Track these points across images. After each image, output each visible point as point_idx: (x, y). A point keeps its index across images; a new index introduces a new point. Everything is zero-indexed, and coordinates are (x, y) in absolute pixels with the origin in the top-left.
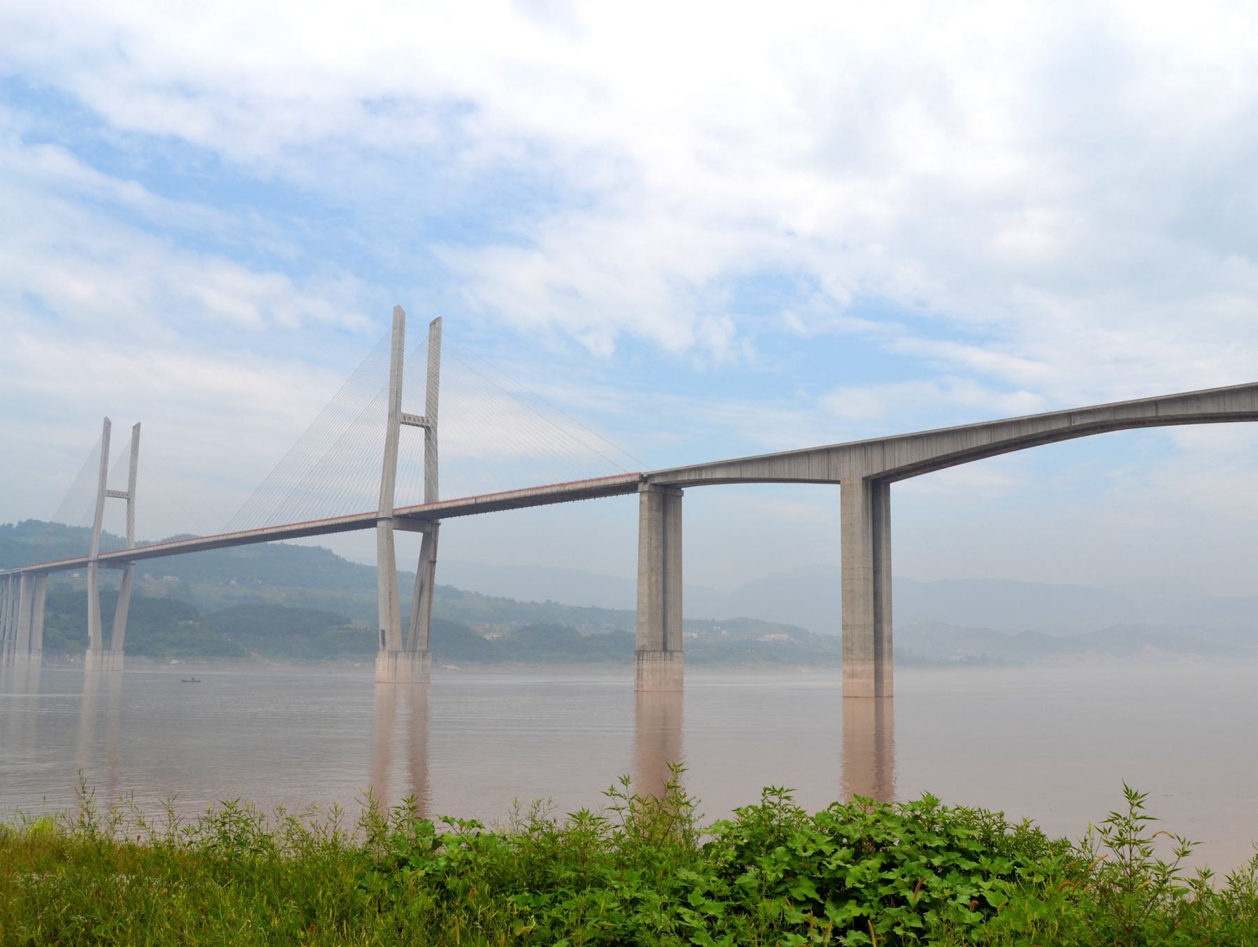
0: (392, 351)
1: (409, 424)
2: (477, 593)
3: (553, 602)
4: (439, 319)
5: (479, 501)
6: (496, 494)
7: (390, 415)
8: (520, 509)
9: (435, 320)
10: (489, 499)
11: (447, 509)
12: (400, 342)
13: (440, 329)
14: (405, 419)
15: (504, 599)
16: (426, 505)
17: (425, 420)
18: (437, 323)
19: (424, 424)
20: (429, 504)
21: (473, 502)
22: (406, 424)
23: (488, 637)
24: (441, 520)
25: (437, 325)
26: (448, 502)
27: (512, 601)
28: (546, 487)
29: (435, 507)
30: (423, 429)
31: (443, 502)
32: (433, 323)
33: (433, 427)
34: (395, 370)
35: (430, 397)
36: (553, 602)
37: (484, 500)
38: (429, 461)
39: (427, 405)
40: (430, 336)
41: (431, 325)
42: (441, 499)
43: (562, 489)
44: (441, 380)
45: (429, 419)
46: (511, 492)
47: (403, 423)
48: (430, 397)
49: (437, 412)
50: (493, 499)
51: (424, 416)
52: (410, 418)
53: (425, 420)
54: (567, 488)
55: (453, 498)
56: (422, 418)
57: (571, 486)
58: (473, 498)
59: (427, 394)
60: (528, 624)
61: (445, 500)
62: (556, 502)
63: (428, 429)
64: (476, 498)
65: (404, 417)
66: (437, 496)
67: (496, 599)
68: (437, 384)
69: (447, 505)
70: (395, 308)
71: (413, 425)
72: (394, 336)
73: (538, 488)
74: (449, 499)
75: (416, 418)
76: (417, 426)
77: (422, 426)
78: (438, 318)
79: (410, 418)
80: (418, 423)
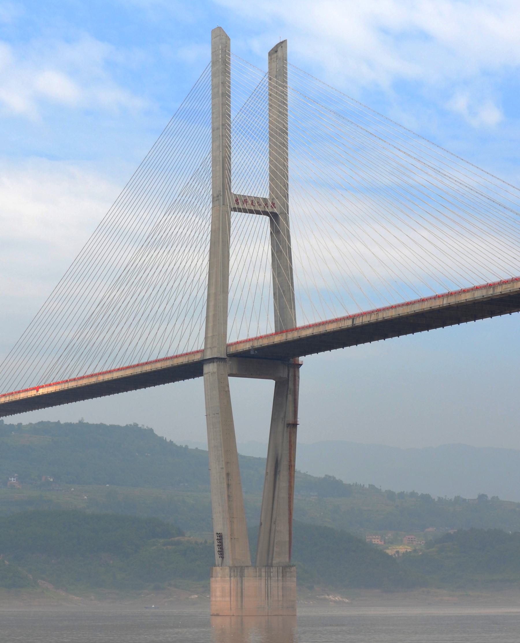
0: (213, 98)
1: (245, 211)
2: (372, 487)
3: (490, 498)
4: (282, 44)
5: (359, 322)
6: (384, 309)
7: (215, 199)
8: (425, 332)
9: (277, 46)
10: (373, 318)
11: (308, 339)
12: (223, 83)
13: (284, 59)
14: (238, 204)
15: (413, 494)
16: (276, 333)
17: (270, 203)
18: (279, 49)
19: (267, 210)
20: (282, 332)
21: (348, 323)
22: (240, 210)
23: (390, 552)
24: (301, 359)
25: (280, 53)
26: (309, 327)
27: (426, 498)
28: (464, 291)
29: (291, 336)
30: (268, 218)
31: (304, 328)
32: (274, 51)
33: (282, 213)
34: (218, 129)
35: (276, 166)
36: (490, 498)
37: (366, 320)
38: (279, 267)
39: (271, 179)
40: (270, 72)
41: (270, 54)
42: (300, 323)
43: (490, 292)
44: (290, 137)
45: (277, 201)
46: (408, 304)
47: (235, 210)
48: (276, 166)
49: (287, 189)
50: (381, 316)
51: (267, 196)
52: (246, 201)
53: (270, 203)
54: (499, 290)
55: (318, 320)
56: (265, 200)
57: (504, 286)
58: (348, 318)
59: (271, 161)
60: (451, 532)
61: (307, 324)
62: (482, 317)
63: (274, 218)
64: (353, 318)
65: (237, 200)
66: (294, 319)
67: (402, 495)
68: (284, 145)
69: (309, 332)
70: (213, 31)
71: (251, 212)
72: (214, 75)
73: (451, 294)
74: (312, 322)
75: (255, 200)
76: (258, 213)
77: (265, 213)
78: (282, 42)
79: (246, 201)
80: (259, 209)
